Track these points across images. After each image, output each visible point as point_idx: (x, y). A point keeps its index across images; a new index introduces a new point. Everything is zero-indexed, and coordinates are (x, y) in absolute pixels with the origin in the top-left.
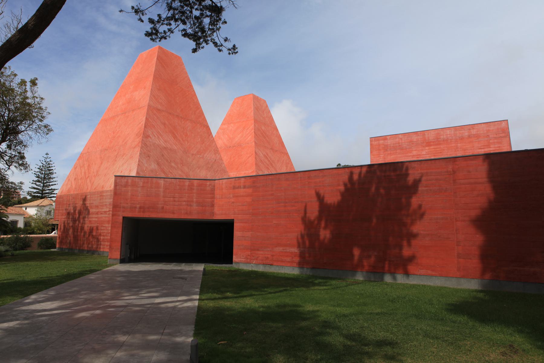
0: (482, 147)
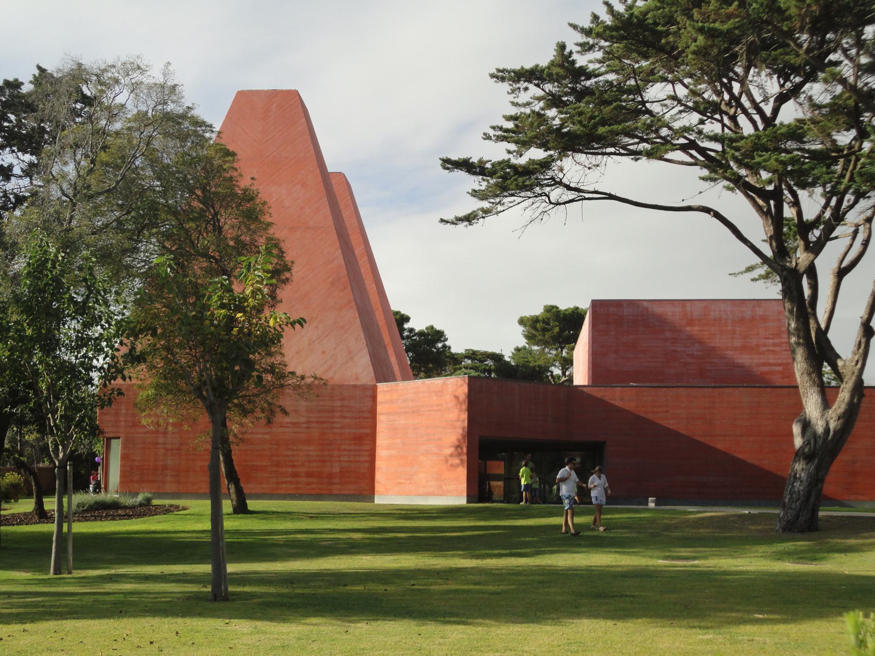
0: (771, 336)
